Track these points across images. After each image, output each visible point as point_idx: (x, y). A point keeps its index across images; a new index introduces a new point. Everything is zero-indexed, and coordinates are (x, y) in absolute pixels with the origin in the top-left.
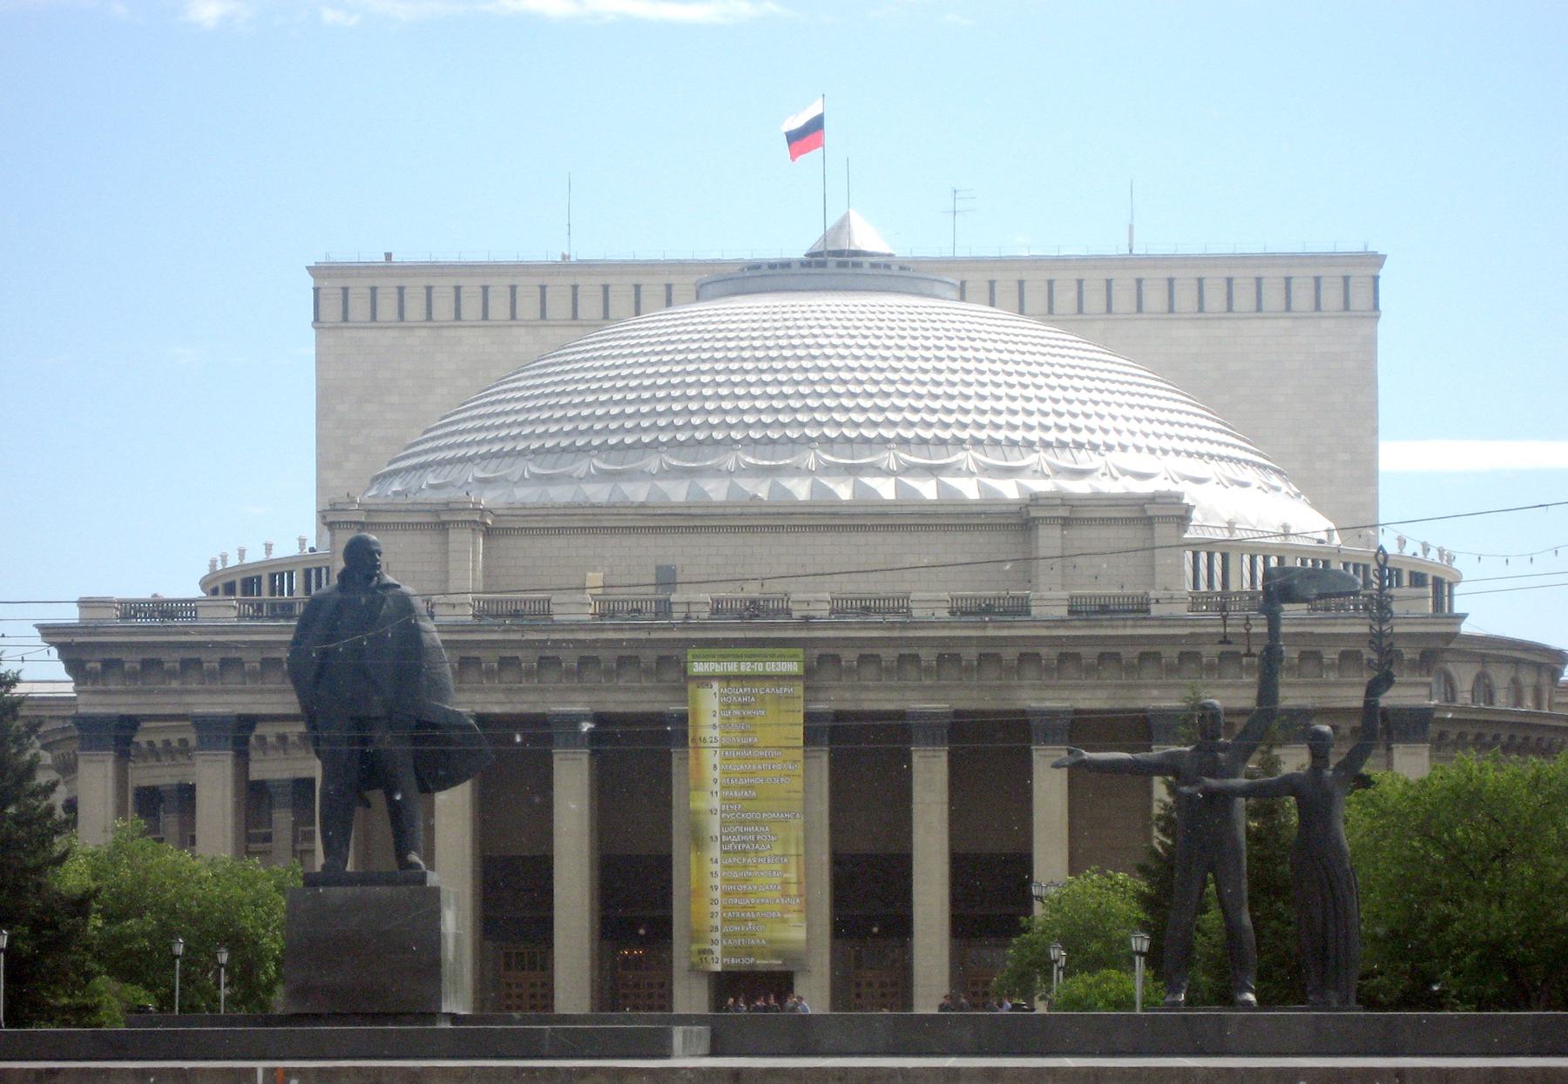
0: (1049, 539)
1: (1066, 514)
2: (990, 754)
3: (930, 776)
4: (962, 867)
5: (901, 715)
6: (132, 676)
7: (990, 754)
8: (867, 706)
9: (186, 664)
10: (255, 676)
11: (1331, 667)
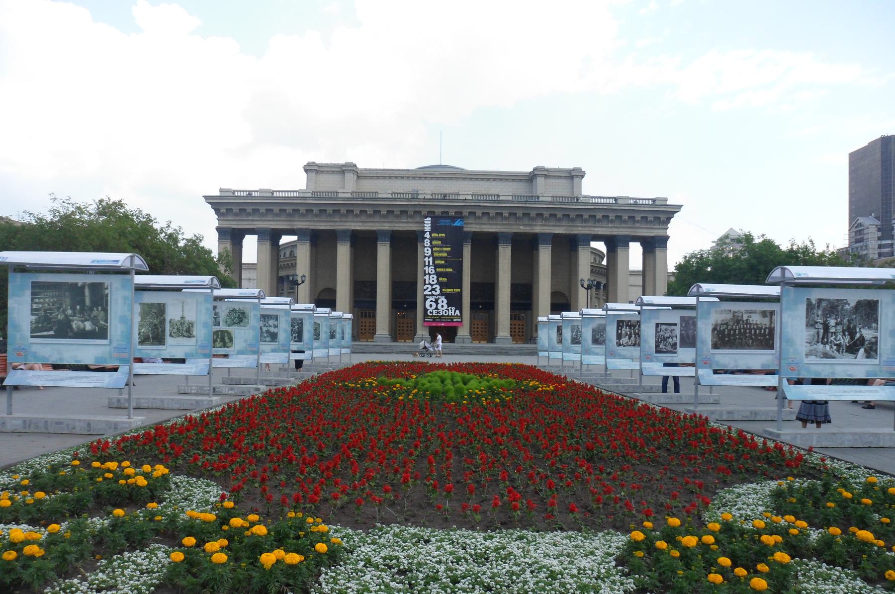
0: (540, 181)
1: (546, 173)
2: (525, 247)
3: (505, 254)
4: (514, 287)
5: (496, 233)
6: (236, 214)
7: (525, 247)
8: (484, 230)
9: (254, 210)
10: (277, 215)
11: (638, 222)
